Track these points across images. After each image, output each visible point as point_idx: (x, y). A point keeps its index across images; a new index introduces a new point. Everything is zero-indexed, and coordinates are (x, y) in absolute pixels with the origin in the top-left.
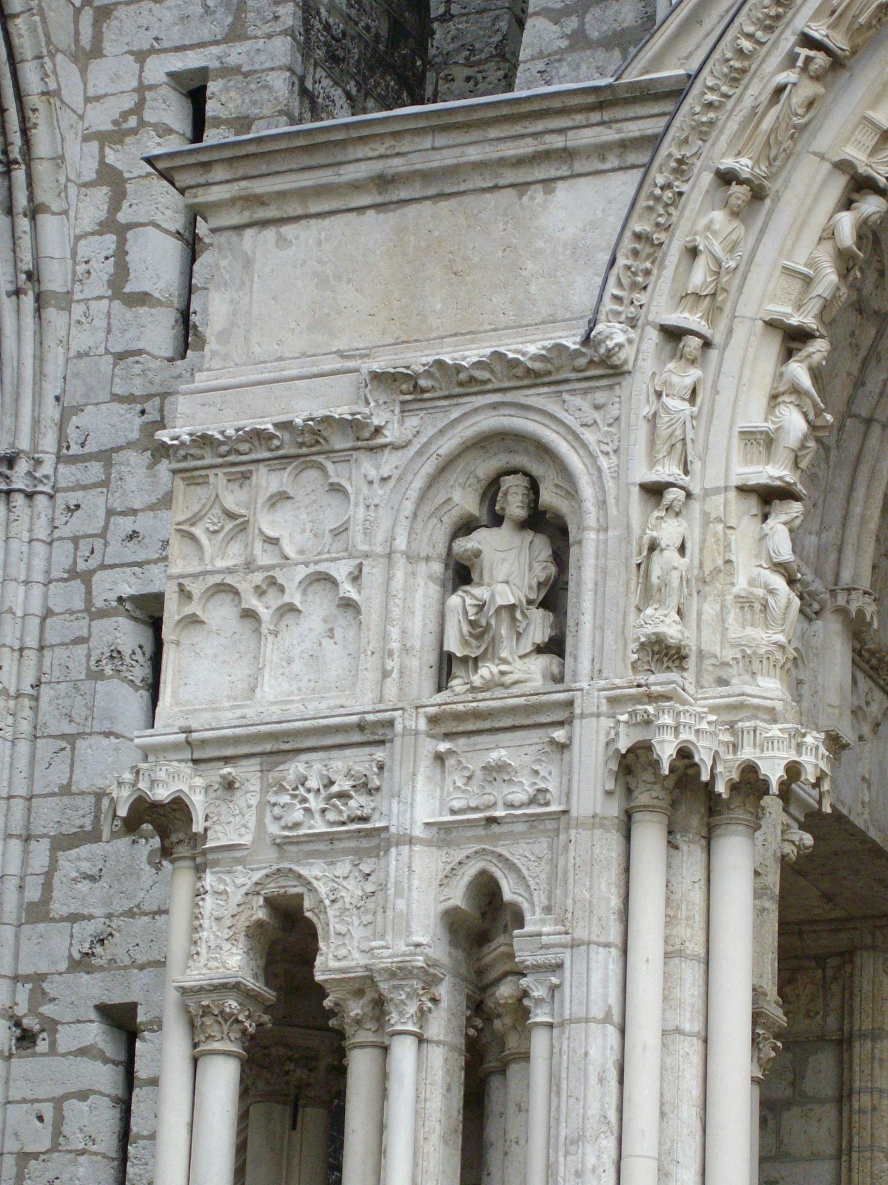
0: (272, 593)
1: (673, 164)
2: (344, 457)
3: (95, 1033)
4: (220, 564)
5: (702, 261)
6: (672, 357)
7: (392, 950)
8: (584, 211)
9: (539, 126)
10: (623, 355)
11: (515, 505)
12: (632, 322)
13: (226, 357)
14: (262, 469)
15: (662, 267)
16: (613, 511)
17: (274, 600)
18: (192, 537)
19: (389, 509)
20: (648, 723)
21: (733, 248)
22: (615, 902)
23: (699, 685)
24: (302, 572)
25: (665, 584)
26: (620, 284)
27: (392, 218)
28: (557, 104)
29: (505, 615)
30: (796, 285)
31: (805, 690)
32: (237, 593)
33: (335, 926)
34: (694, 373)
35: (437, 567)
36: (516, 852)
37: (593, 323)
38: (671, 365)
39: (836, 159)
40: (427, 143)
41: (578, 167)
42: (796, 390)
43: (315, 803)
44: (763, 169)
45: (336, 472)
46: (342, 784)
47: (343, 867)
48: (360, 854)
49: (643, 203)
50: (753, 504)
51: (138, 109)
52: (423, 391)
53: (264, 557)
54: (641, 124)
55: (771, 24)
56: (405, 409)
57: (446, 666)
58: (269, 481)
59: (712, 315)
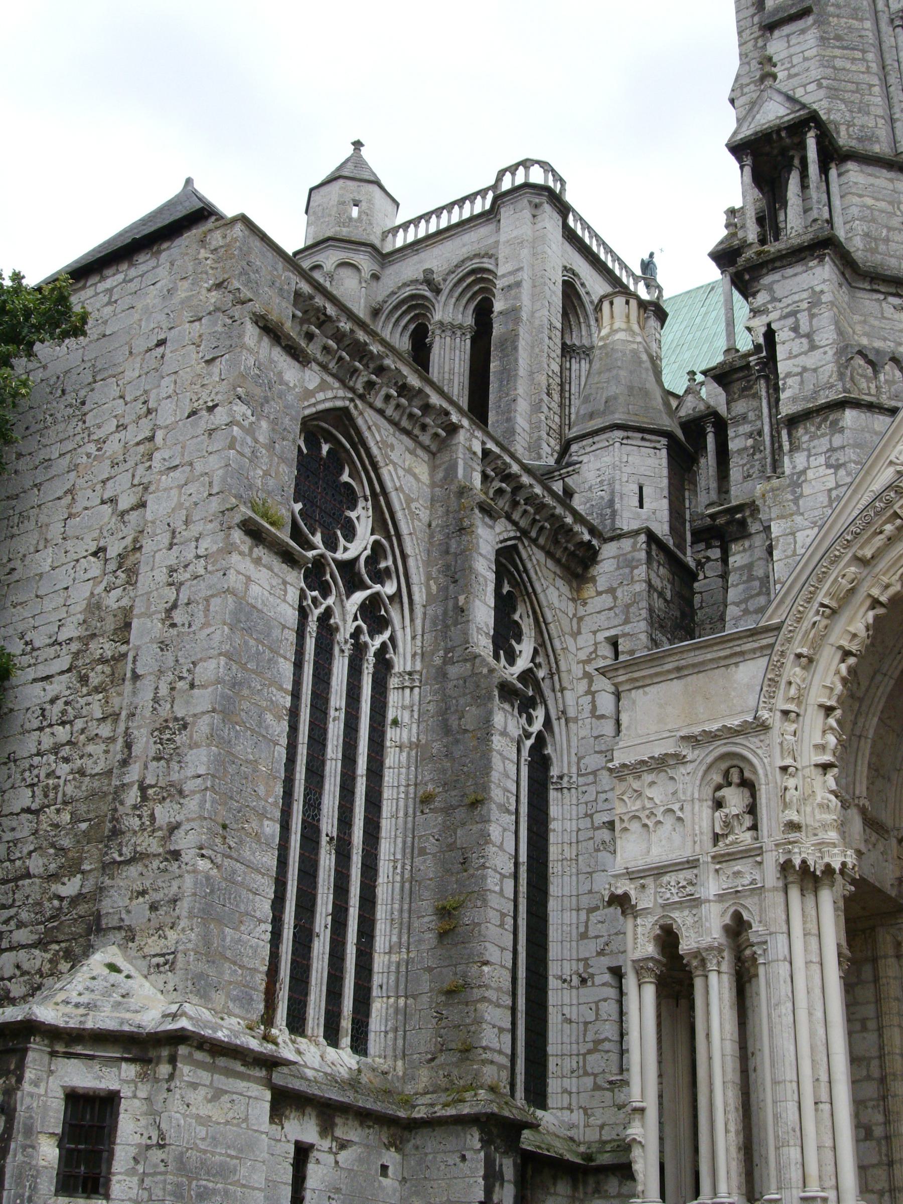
2: (673, 767)
3: (607, 977)
4: (634, 808)
5: (793, 687)
7: (706, 941)
8: (750, 672)
9: (731, 644)
11: (735, 779)
12: (771, 710)
16: (770, 777)
17: (653, 819)
19: (690, 784)
21: (804, 680)
22: (784, 917)
24: (662, 809)
25: (791, 801)
27: (683, 681)
30: (828, 691)
33: (685, 933)
34: (795, 726)
35: (710, 803)
36: (748, 902)
37: (757, 711)
41: (746, 657)
42: (832, 728)
43: (674, 891)
44: (811, 652)
46: (683, 883)
47: (686, 913)
48: (692, 907)
49: (770, 667)
50: (820, 770)
51: (595, 651)
53: (648, 805)
55: (809, 601)
56: (693, 748)
57: (716, 838)
58: (648, 778)
59: (799, 705)
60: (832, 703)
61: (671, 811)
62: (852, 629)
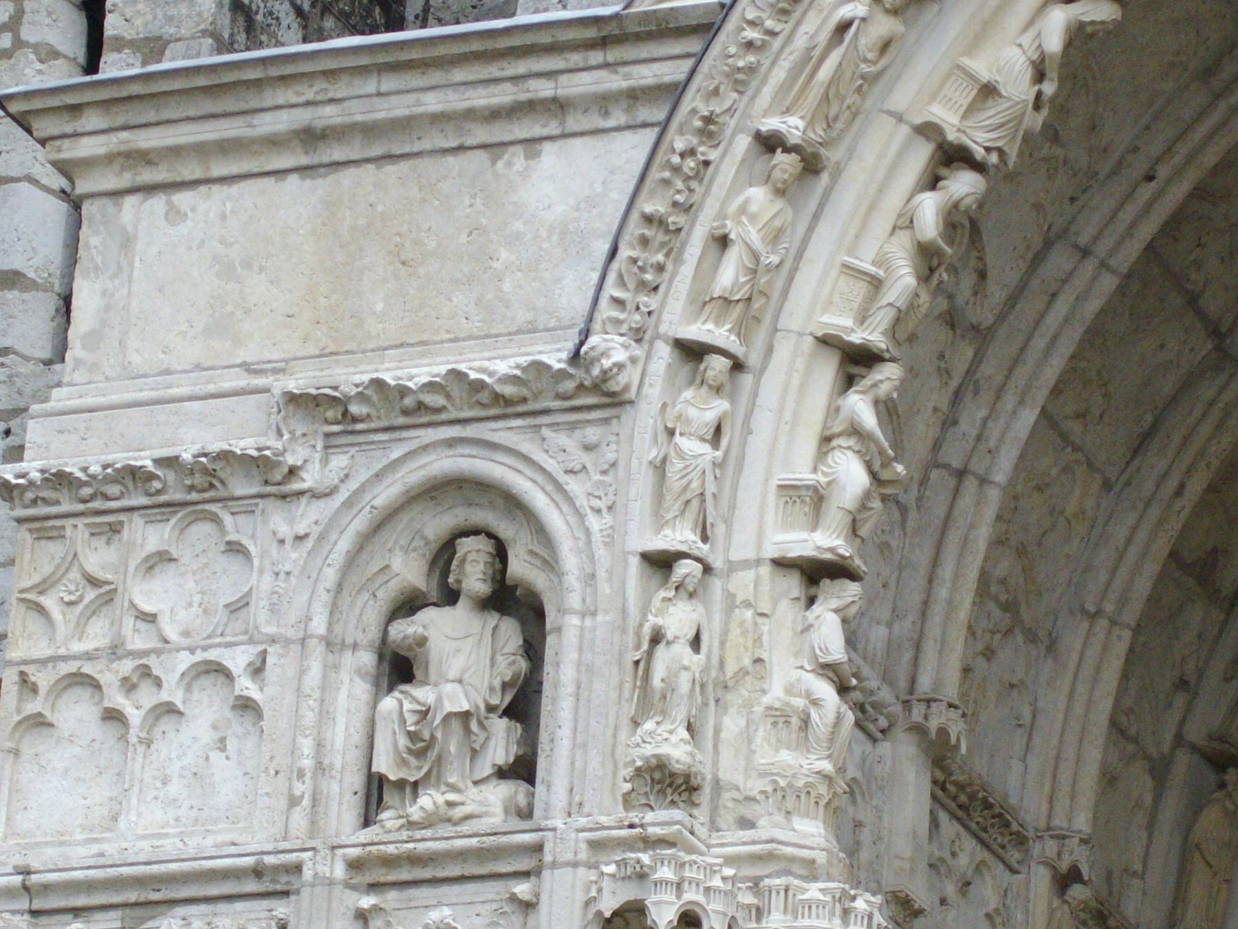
0: (145, 688)
1: (698, 123)
2: (246, 506)
4: (77, 647)
6: (691, 383)
8: (577, 182)
10: (622, 379)
11: (474, 577)
12: (638, 335)
13: (94, 368)
14: (137, 520)
15: (679, 261)
17: (147, 697)
18: (40, 610)
19: (296, 578)
20: (642, 876)
21: (775, 237)
23: (714, 827)
24: (184, 661)
26: (621, 282)
28: (545, 38)
29: (456, 725)
30: (860, 289)
31: (866, 835)
32: (97, 686)
34: (720, 406)
35: (367, 659)
37: (586, 334)
38: (688, 394)
39: (918, 121)
40: (370, 86)
41: (572, 124)
42: (855, 431)
44: (820, 131)
45: (235, 526)
49: (655, 174)
50: (793, 584)
52: (355, 420)
54: (657, 68)
56: (330, 443)
57: (376, 793)
58: (150, 536)
60: (872, 335)
61: (218, 670)
62: (982, 67)
